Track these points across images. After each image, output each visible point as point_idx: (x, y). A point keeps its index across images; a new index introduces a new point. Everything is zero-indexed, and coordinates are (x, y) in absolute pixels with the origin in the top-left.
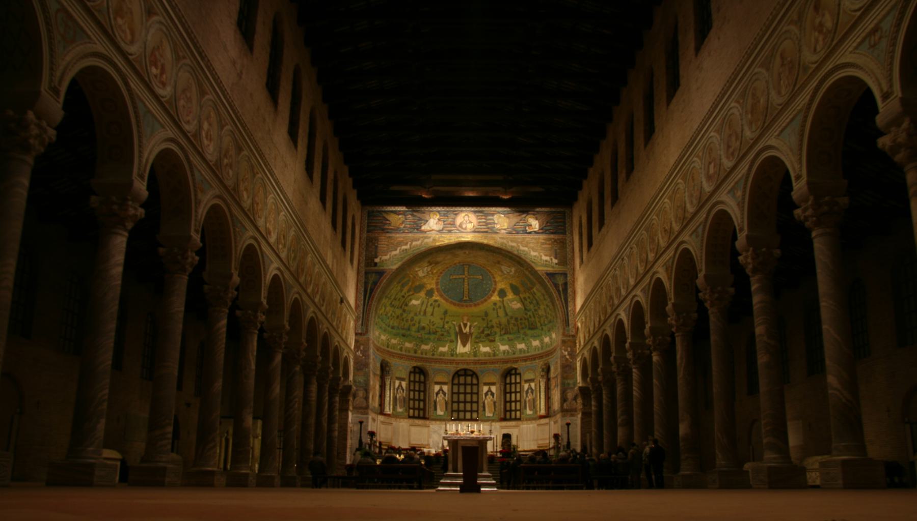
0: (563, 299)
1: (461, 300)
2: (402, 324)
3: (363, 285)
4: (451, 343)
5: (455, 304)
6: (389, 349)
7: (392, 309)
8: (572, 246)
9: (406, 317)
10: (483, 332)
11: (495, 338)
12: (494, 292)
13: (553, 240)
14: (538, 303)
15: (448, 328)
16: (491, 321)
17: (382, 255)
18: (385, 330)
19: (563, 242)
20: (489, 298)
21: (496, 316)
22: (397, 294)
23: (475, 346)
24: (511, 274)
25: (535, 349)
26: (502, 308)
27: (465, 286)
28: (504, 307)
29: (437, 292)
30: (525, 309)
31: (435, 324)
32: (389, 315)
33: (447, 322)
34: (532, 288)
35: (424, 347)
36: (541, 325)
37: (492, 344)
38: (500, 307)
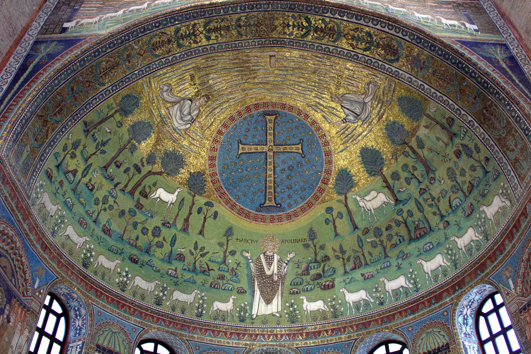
0: (517, 81)
1: (261, 207)
2: (134, 237)
3: (21, 61)
4: (240, 296)
5: (247, 216)
6: (88, 272)
7: (108, 186)
8: (496, 11)
9: (141, 223)
10: (307, 271)
11: (333, 282)
12: (325, 182)
13: (455, 4)
14: (429, 169)
15: (235, 266)
16: (322, 247)
17: (83, 19)
18: (82, 223)
19: (476, 7)
20: (316, 198)
21: (333, 234)
22: (121, 151)
23: (293, 301)
24: (363, 117)
25: (436, 277)
26: (345, 215)
27: (269, 173)
28: (349, 212)
29: (213, 183)
30: (397, 201)
31: (208, 252)
32: (100, 194)
33: (233, 253)
34: (415, 130)
35: (178, 295)
36: (442, 216)
37: (327, 292)
38: (340, 215)
